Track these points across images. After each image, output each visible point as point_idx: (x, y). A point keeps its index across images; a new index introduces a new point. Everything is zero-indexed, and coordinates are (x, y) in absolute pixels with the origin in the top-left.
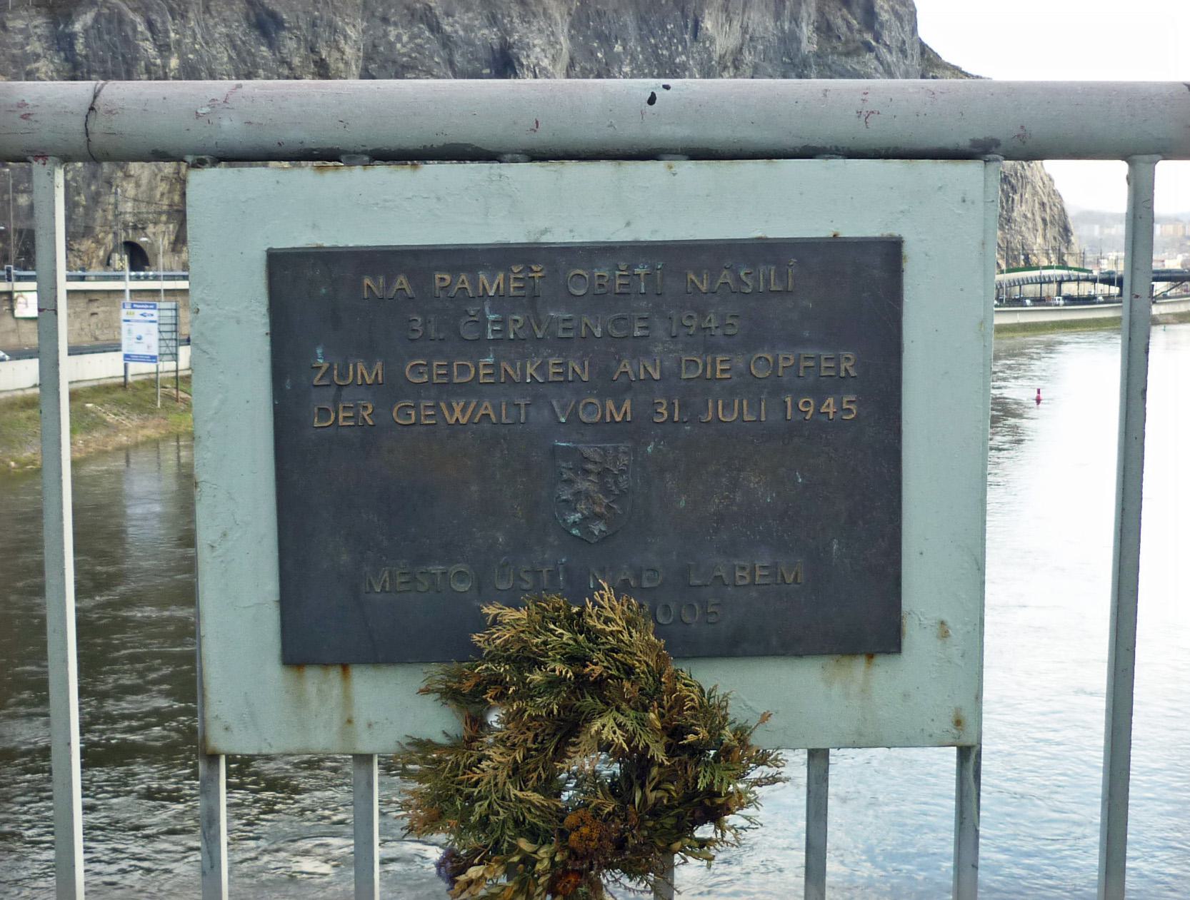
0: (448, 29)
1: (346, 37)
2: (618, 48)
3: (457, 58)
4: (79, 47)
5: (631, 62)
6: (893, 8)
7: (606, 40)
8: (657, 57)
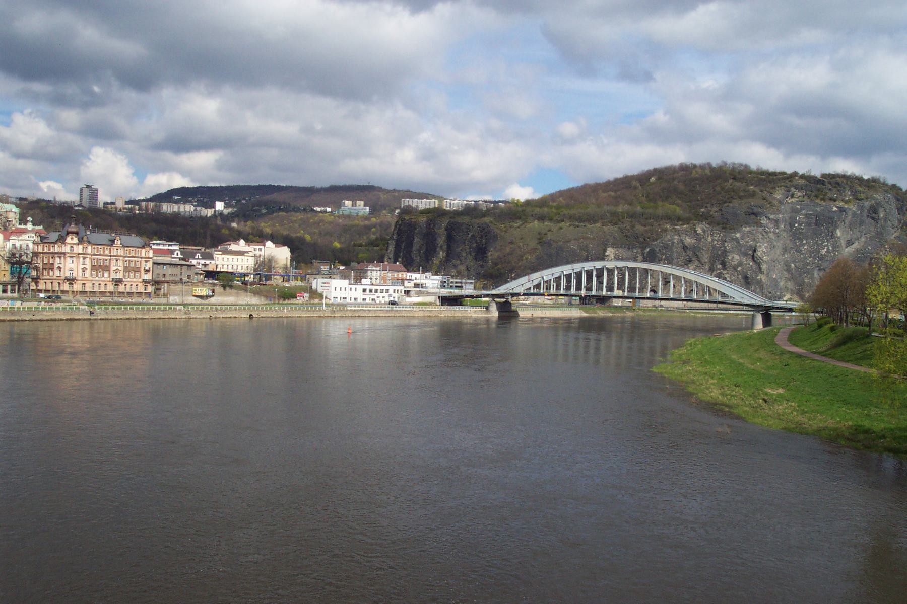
1: (703, 250)
2: (804, 242)
3: (743, 249)
4: (645, 255)
7: (801, 240)
8: (816, 243)
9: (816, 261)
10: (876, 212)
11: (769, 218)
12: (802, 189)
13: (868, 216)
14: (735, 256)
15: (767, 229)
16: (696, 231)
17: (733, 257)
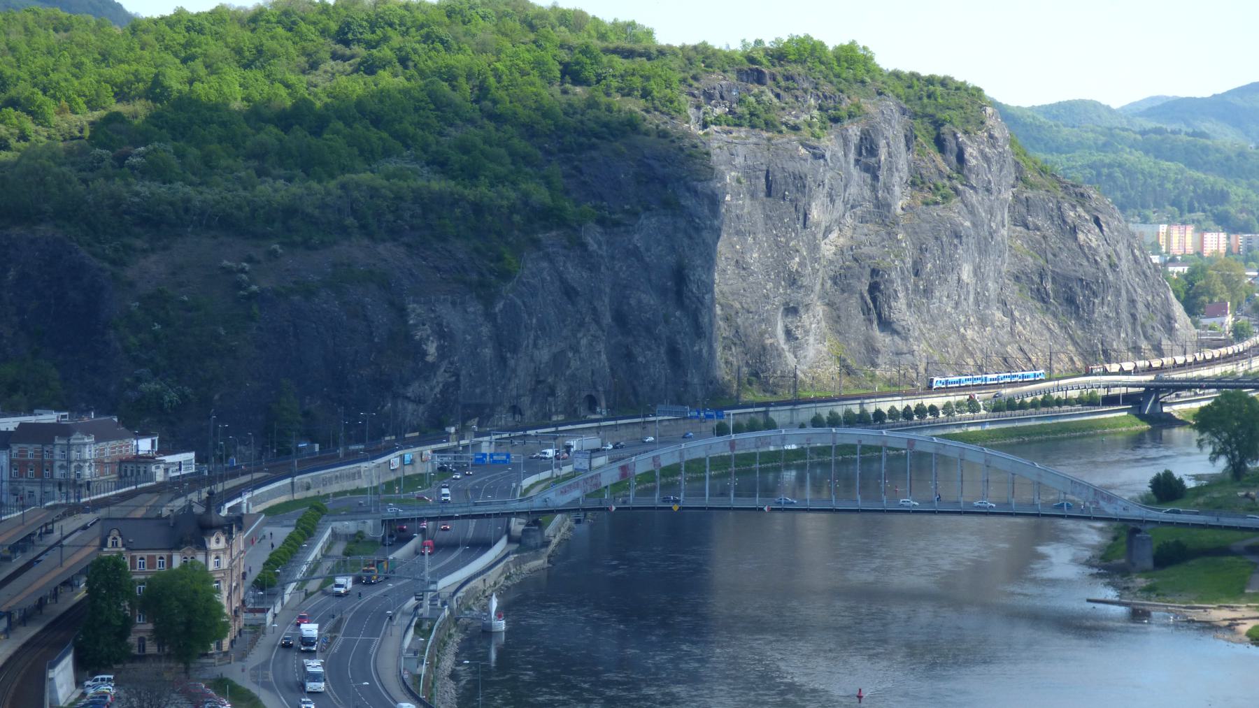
0: (648, 259)
2: (750, 240)
4: (499, 321)
5: (759, 249)
6: (982, 152)
8: (777, 244)
9: (781, 291)
10: (873, 151)
11: (696, 192)
12: (722, 97)
13: (857, 161)
14: (643, 296)
15: (697, 220)
16: (583, 246)
17: (640, 301)
